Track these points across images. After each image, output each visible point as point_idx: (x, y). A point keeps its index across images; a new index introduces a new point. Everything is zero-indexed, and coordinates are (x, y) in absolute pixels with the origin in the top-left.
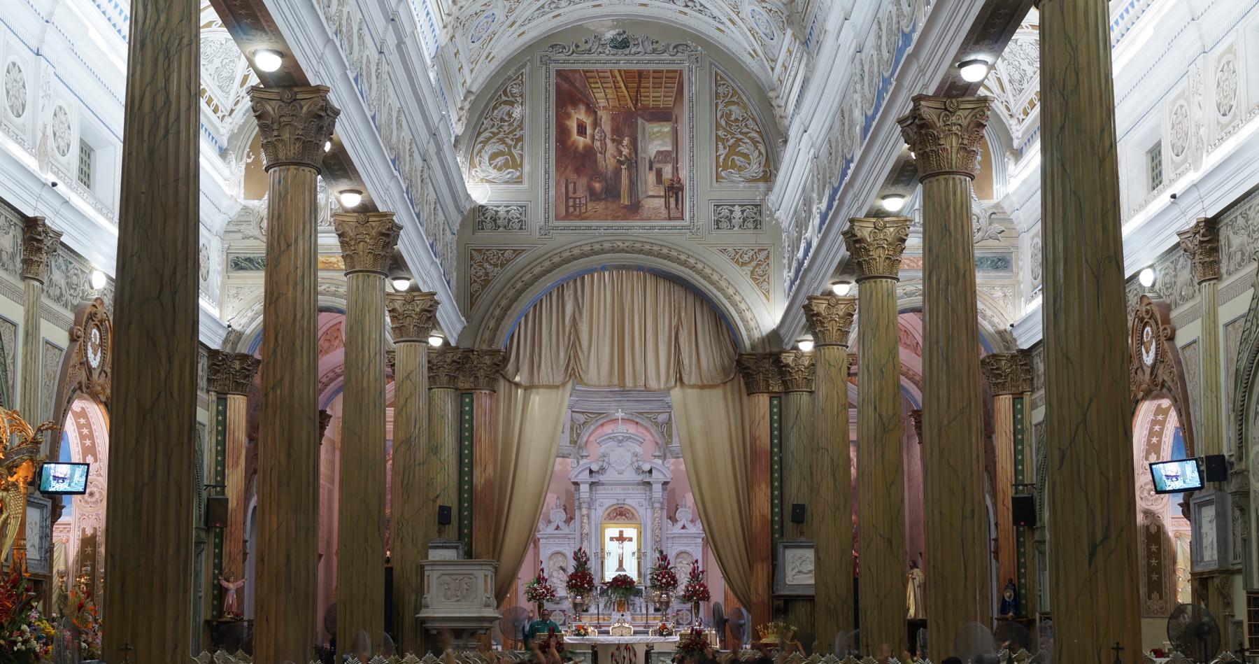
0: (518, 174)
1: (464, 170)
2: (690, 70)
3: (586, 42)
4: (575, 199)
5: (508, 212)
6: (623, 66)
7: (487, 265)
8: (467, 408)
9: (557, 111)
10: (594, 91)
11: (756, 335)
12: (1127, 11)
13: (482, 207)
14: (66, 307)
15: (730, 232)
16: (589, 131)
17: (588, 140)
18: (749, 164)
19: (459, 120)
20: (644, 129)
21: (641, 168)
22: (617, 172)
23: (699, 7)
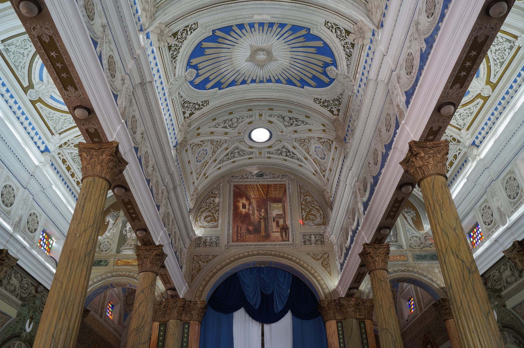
0: (216, 224)
1: (193, 223)
2: (289, 184)
3: (246, 175)
4: (241, 234)
5: (211, 239)
6: (261, 183)
7: (200, 262)
8: (186, 331)
9: (234, 200)
11: (327, 291)
12: (480, 133)
13: (200, 237)
14: (17, 297)
15: (311, 246)
16: (247, 207)
17: (247, 210)
18: (316, 218)
19: (192, 200)
20: (271, 206)
21: (269, 221)
22: (259, 223)
23: (292, 155)
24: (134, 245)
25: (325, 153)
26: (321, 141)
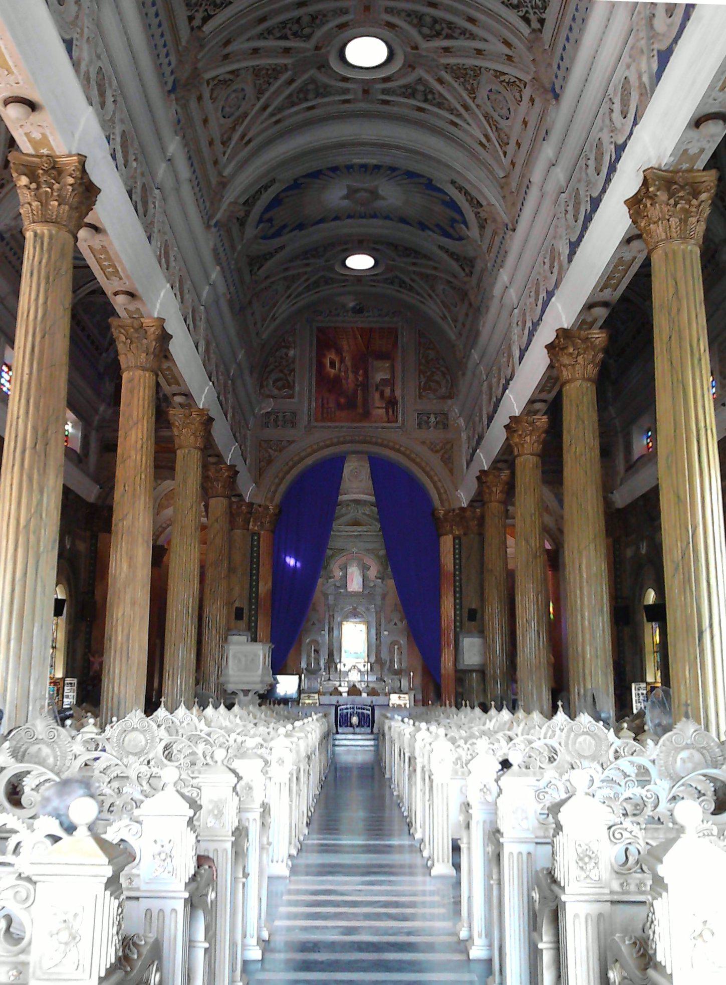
7: (270, 450)
17: (337, 371)
22: (355, 392)
25: (510, 105)
26: (502, 78)
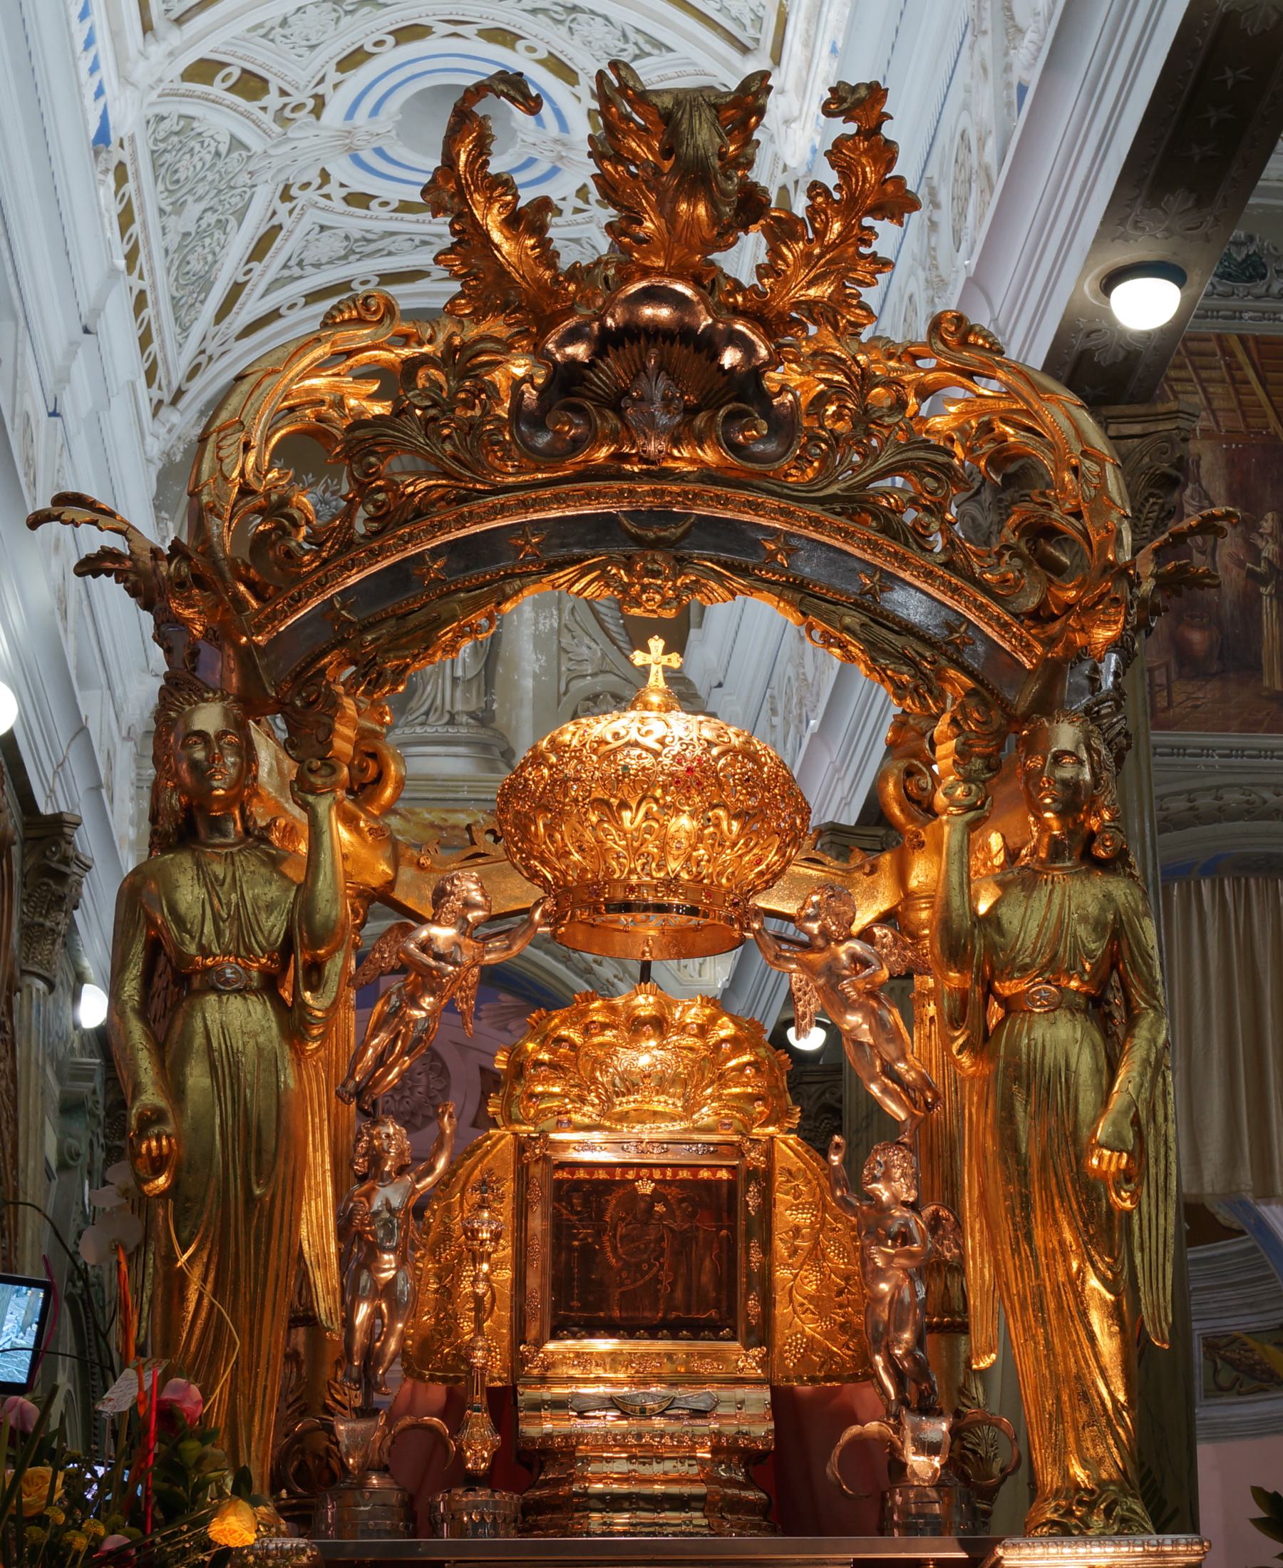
6: (1252, 326)
10: (1178, 387)
22: (1249, 604)
24: (471, 715)
